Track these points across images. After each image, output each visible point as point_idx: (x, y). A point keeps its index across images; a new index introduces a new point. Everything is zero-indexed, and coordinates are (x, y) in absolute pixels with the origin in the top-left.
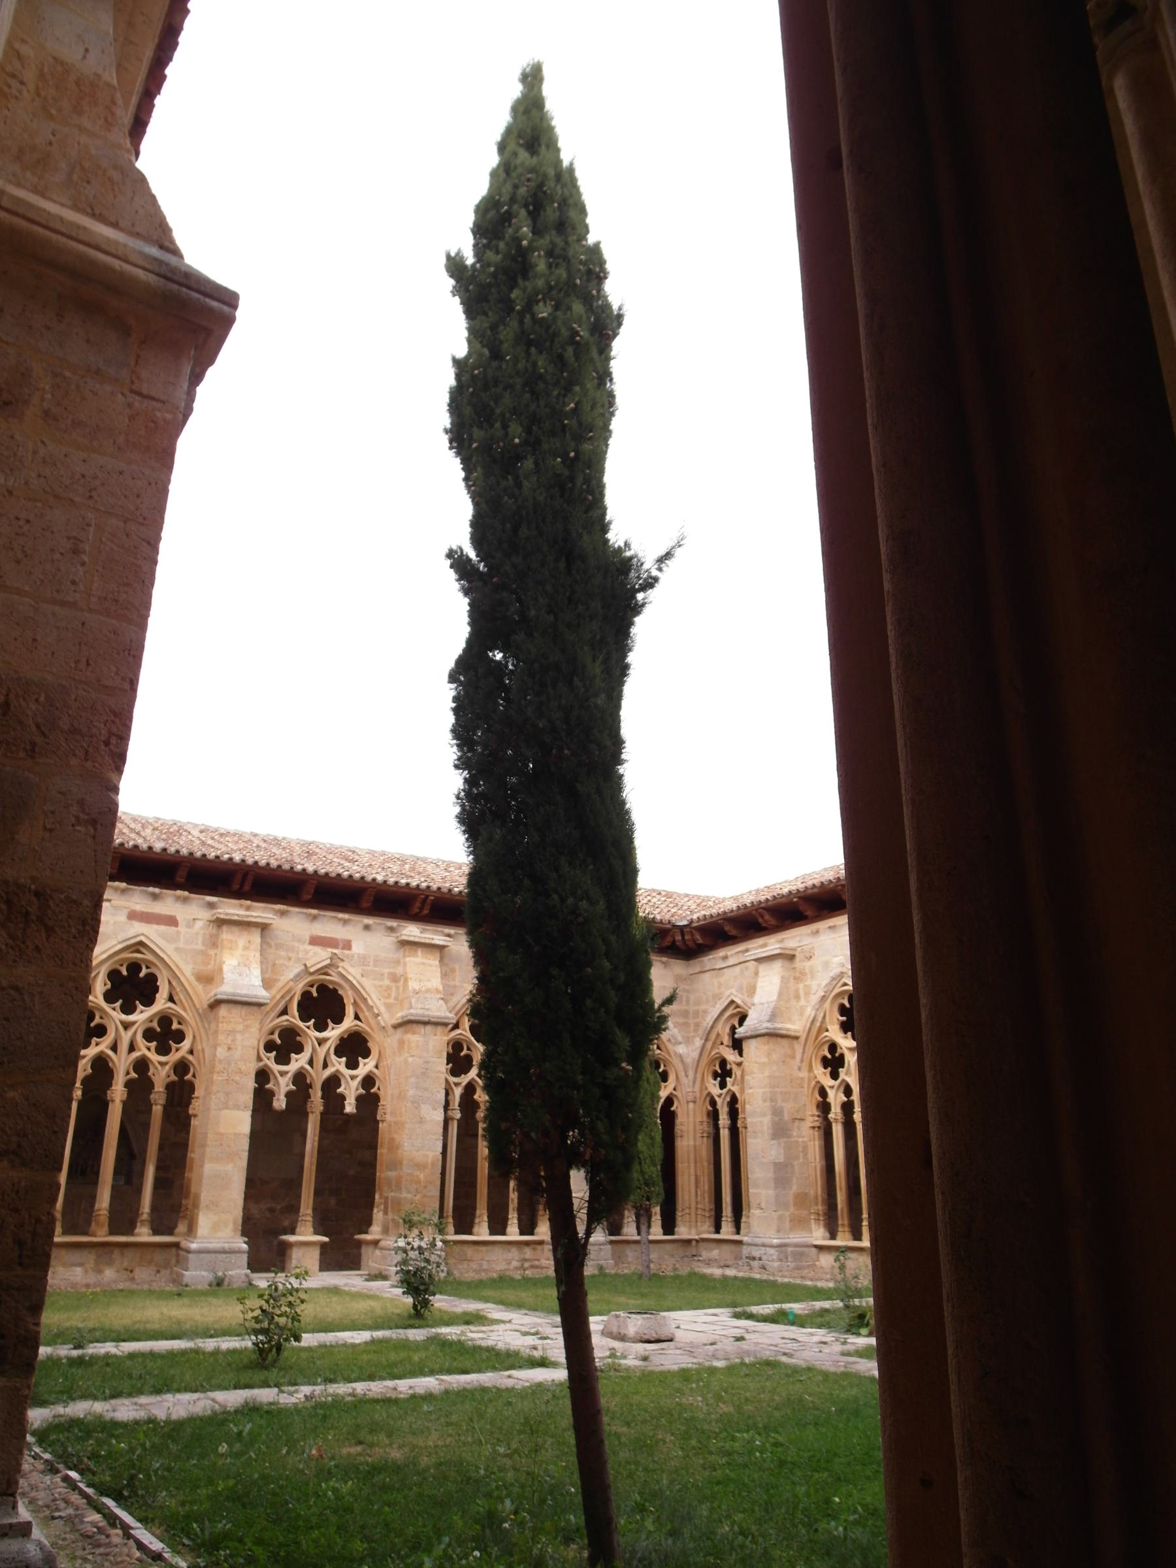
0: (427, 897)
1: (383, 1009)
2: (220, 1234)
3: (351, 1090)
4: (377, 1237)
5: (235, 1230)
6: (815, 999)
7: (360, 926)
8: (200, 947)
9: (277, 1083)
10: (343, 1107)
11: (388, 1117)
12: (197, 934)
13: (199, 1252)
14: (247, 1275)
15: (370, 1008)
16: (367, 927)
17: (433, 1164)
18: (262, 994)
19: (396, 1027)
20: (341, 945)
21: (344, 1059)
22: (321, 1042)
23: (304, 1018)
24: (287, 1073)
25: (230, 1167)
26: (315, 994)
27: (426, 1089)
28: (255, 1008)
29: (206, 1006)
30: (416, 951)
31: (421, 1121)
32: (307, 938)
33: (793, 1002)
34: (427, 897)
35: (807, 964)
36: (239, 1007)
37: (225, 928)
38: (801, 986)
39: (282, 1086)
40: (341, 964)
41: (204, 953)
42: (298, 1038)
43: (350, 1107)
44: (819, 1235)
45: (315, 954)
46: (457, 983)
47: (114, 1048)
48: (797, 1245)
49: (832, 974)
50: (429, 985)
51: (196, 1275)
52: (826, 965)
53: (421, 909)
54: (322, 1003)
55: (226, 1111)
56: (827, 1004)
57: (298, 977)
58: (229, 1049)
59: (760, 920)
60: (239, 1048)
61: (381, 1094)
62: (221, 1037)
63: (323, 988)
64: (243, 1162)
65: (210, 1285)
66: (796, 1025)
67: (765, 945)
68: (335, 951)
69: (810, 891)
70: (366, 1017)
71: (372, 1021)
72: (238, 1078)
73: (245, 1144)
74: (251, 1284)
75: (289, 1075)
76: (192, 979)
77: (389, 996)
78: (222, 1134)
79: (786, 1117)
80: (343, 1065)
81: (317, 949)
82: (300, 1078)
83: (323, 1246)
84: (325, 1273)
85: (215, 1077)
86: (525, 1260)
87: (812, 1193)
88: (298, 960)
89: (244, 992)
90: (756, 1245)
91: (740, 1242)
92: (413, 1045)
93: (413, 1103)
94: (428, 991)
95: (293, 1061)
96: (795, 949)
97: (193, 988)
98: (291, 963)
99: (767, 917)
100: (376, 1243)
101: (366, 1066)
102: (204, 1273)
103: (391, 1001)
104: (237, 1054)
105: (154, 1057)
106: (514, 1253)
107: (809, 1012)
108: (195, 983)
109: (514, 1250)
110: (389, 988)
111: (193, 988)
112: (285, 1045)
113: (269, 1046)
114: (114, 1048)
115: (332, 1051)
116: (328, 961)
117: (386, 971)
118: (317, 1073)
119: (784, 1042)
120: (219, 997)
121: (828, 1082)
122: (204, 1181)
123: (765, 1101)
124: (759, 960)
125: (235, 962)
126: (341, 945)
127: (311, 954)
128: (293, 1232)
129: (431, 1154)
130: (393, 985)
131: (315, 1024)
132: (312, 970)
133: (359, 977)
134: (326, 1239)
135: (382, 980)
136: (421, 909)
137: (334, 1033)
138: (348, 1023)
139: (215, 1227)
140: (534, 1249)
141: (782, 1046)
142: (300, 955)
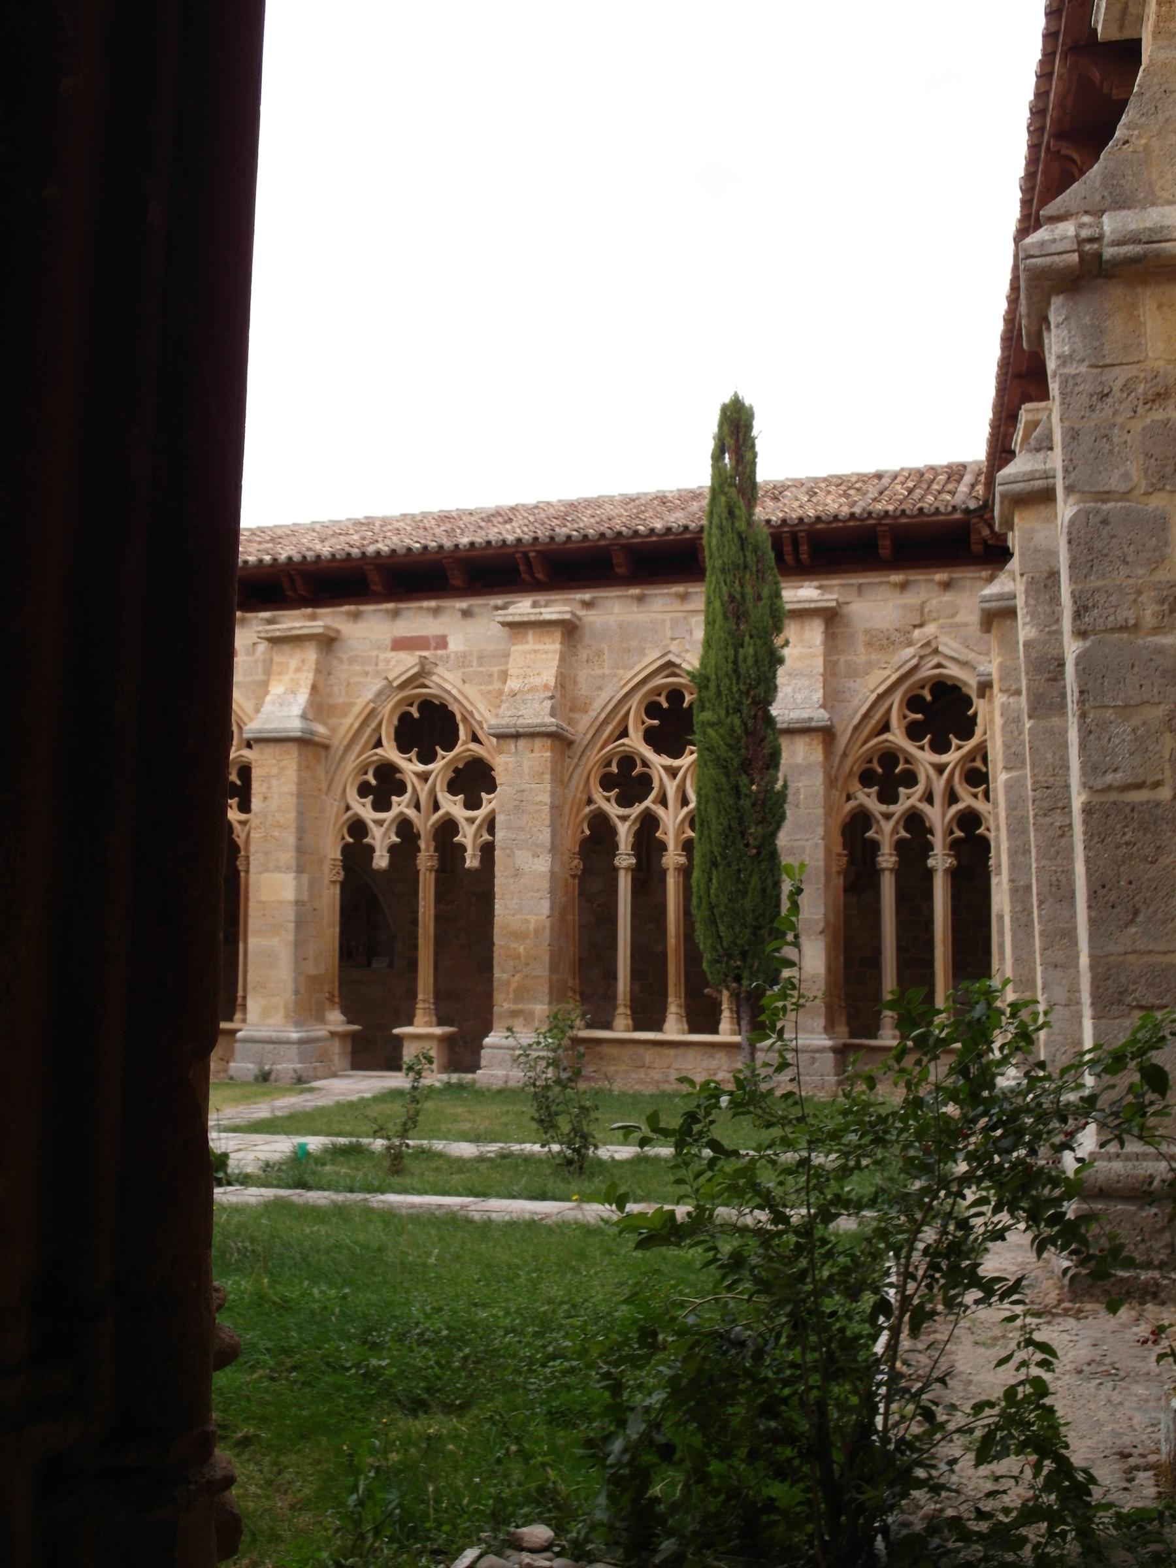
5: (287, 1016)
9: (880, 831)
16: (466, 614)
17: (536, 932)
20: (433, 644)
23: (403, 748)
25: (275, 942)
27: (521, 829)
30: (526, 635)
32: (388, 642)
36: (272, 745)
39: (381, 839)
42: (398, 776)
46: (607, 671)
47: (929, 798)
54: (428, 724)
55: (267, 875)
58: (265, 798)
60: (276, 796)
68: (425, 653)
72: (277, 834)
75: (895, 818)
78: (265, 902)
82: (405, 827)
88: (377, 673)
93: (504, 849)
102: (251, 1066)
104: (274, 803)
105: (613, 810)
112: (384, 785)
113: (364, 790)
114: (929, 798)
116: (415, 670)
117: (496, 669)
126: (433, 644)
127: (393, 663)
129: (533, 919)
135: (491, 683)
139: (265, 1013)
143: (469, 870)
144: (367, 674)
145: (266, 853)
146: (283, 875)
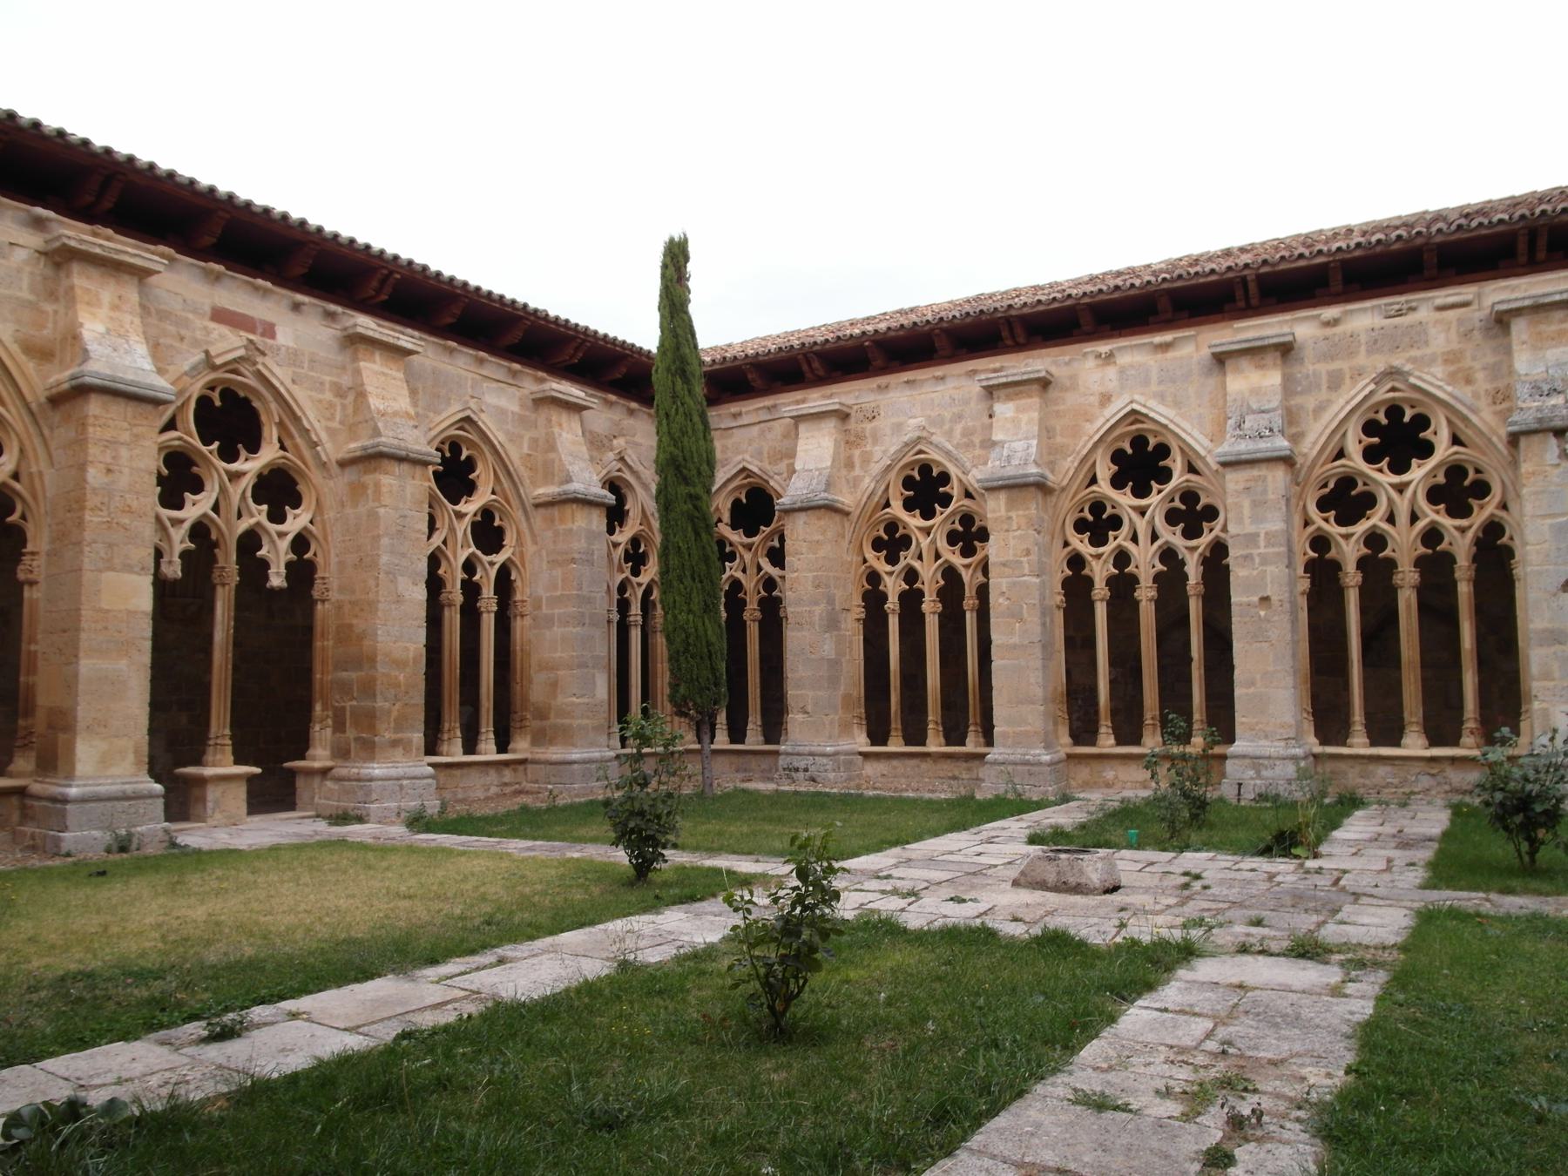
0: (391, 272)
1: (324, 436)
2: (115, 771)
3: (277, 555)
4: (329, 763)
5: (138, 763)
6: (876, 469)
7: (285, 302)
8: (26, 294)
10: (267, 578)
11: (334, 595)
12: (19, 270)
13: (83, 800)
14: (166, 831)
15: (305, 432)
16: (296, 307)
17: (415, 661)
18: (161, 384)
19: (343, 464)
20: (260, 330)
21: (265, 507)
22: (235, 476)
24: (181, 521)
25: (123, 664)
26: (218, 403)
27: (404, 555)
28: (150, 407)
29: (43, 400)
30: (373, 354)
31: (399, 599)
32: (207, 309)
33: (844, 472)
34: (391, 272)
35: (868, 426)
36: (122, 402)
37: (76, 267)
38: (857, 453)
40: (260, 359)
41: (32, 306)
42: (195, 469)
43: (277, 580)
44: (861, 742)
45: (222, 337)
48: (847, 753)
49: (906, 439)
50: (396, 406)
51: (84, 837)
52: (898, 428)
53: (379, 291)
55: (109, 576)
56: (892, 475)
57: (194, 371)
58: (109, 471)
59: (805, 367)
60: (126, 471)
61: (320, 560)
62: (93, 451)
63: (228, 394)
64: (143, 656)
65: (108, 851)
66: (846, 498)
67: (804, 401)
68: (252, 337)
69: (892, 334)
70: (296, 447)
71: (307, 453)
72: (127, 521)
73: (144, 630)
74: (174, 845)
76: (15, 348)
77: (332, 418)
78: (108, 611)
79: (837, 608)
80: (264, 515)
81: (225, 330)
83: (250, 779)
84: (256, 818)
85: (88, 516)
86: (506, 784)
87: (855, 694)
88: (196, 343)
89: (130, 377)
90: (798, 754)
91: (777, 753)
92: (384, 490)
93: (388, 573)
94: (395, 414)
95: (188, 504)
96: (850, 407)
97: (19, 366)
98: (184, 346)
99: (816, 365)
100: (325, 772)
101: (296, 521)
102: (96, 833)
103: (335, 425)
104: (124, 480)
106: (492, 776)
107: (867, 483)
108: (22, 358)
109: (493, 774)
110: (331, 405)
111: (19, 366)
115: (249, 493)
116: (241, 352)
117: (327, 379)
118: (228, 522)
119: (837, 518)
120: (88, 380)
121: (882, 567)
122: (81, 687)
123: (818, 587)
124: (799, 419)
125: (101, 328)
127: (215, 335)
128: (198, 762)
129: (412, 647)
130: (337, 401)
131: (219, 449)
132: (218, 361)
133: (288, 382)
134: (258, 770)
135: (322, 392)
136: (379, 291)
137: (251, 466)
138: (269, 454)
139: (105, 761)
140: (515, 771)
141: (830, 523)
142: (199, 334)
143: (272, 589)
144: (182, 339)
145: (110, 546)
146: (134, 577)
